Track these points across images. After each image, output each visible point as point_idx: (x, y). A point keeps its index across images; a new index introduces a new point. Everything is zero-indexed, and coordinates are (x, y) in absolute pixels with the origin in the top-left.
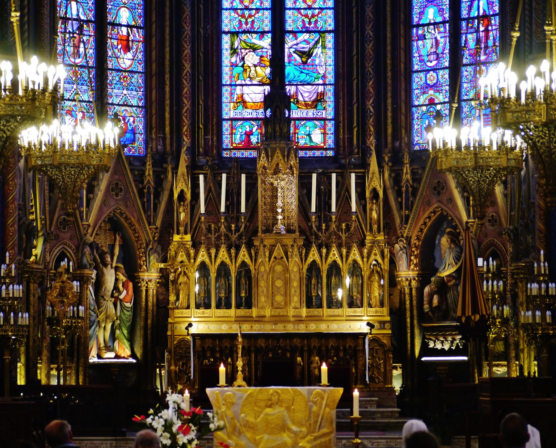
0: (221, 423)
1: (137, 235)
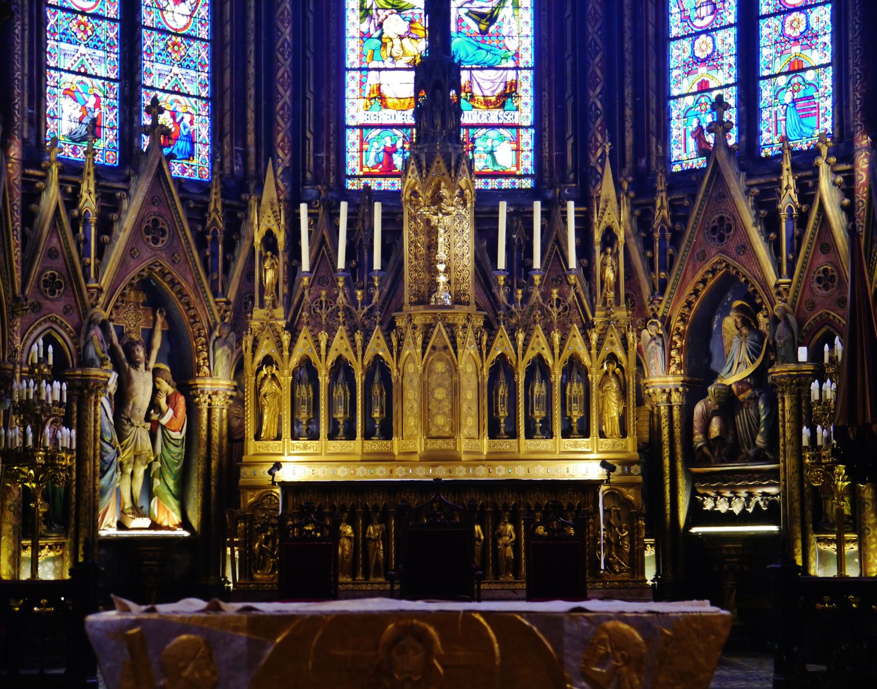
1: (192, 312)
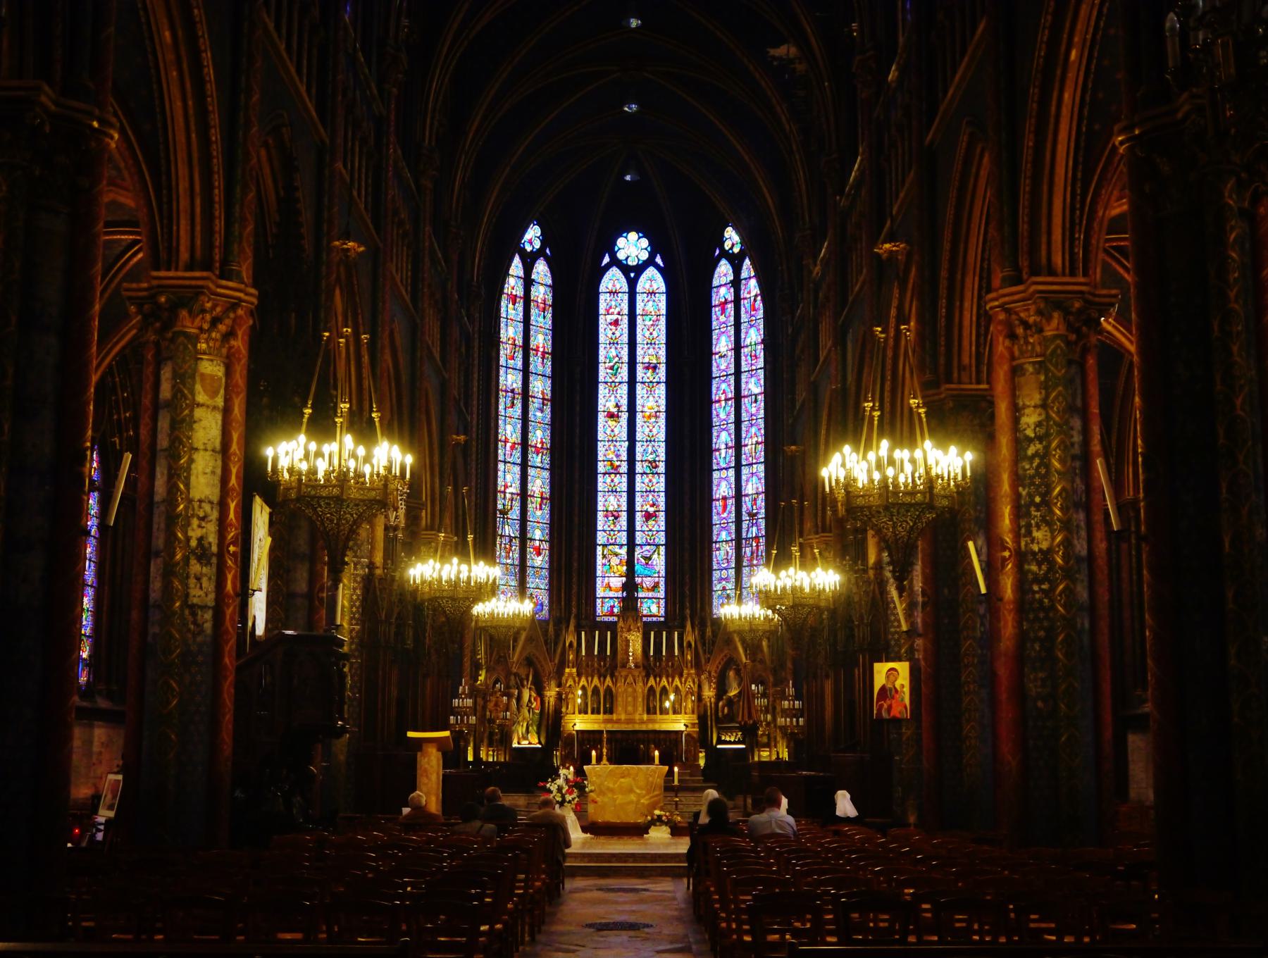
0: (593, 788)
